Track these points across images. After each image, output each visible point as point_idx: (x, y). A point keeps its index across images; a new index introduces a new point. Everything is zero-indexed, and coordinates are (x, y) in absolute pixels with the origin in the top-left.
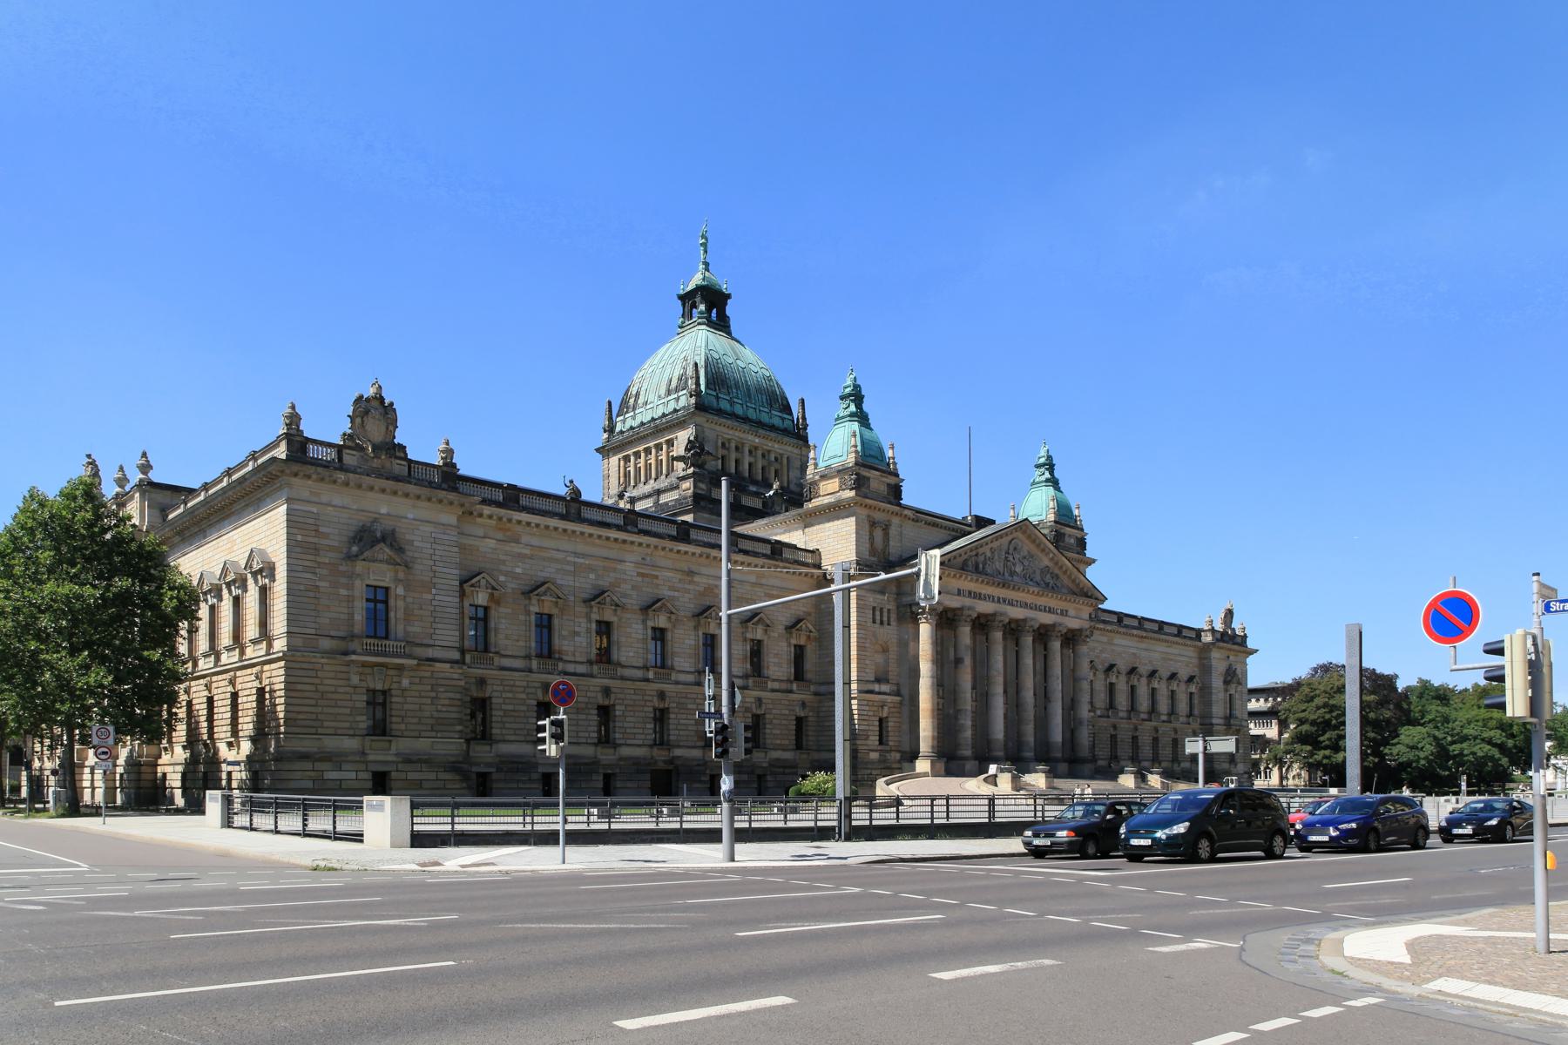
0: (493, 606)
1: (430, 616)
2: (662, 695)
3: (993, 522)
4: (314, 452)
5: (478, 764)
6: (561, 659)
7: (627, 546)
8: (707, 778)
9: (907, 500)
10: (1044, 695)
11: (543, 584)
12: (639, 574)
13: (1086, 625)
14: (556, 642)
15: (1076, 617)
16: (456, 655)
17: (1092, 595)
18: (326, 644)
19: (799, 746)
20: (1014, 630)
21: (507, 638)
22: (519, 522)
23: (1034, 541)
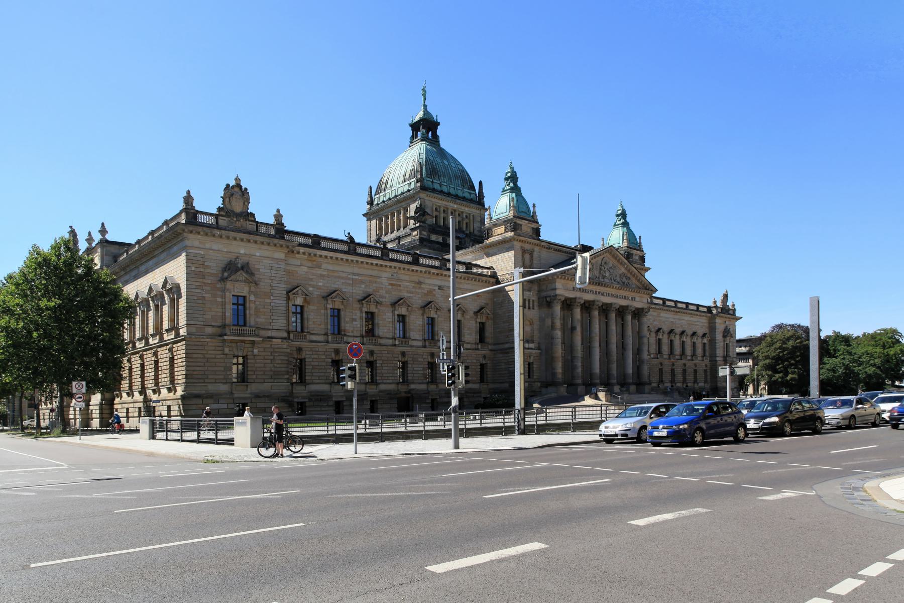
0: (306, 305)
1: (270, 314)
2: (403, 354)
3: (592, 248)
4: (202, 219)
6: (345, 335)
7: (383, 269)
8: (429, 401)
9: (543, 237)
10: (622, 347)
11: (335, 291)
12: (391, 284)
13: (645, 306)
15: (640, 302)
16: (285, 335)
17: (649, 289)
18: (209, 330)
19: (482, 380)
20: (605, 309)
21: (314, 323)
22: (321, 256)
23: (616, 259)
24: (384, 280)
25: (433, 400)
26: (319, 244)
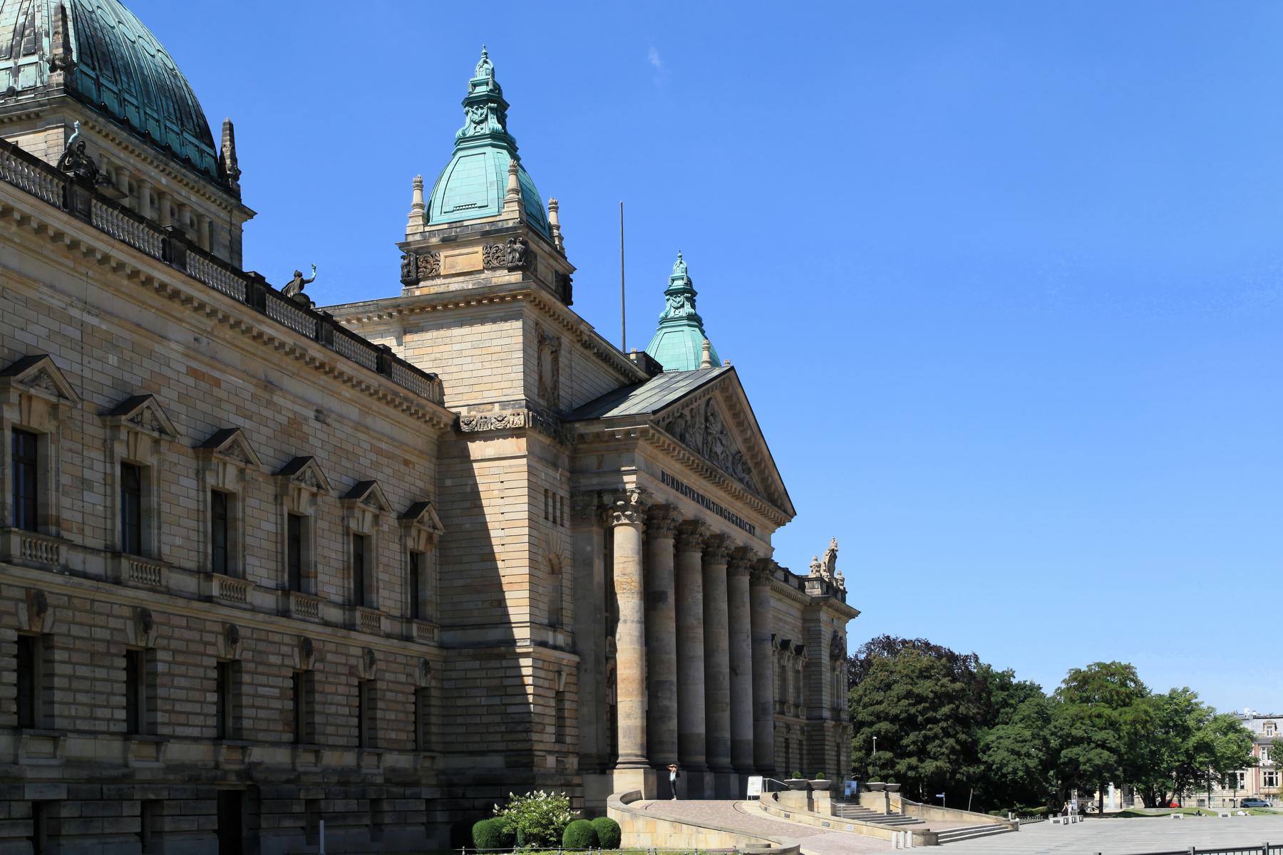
2: (232, 635)
7: (175, 307)
11: (28, 361)
24: (173, 351)
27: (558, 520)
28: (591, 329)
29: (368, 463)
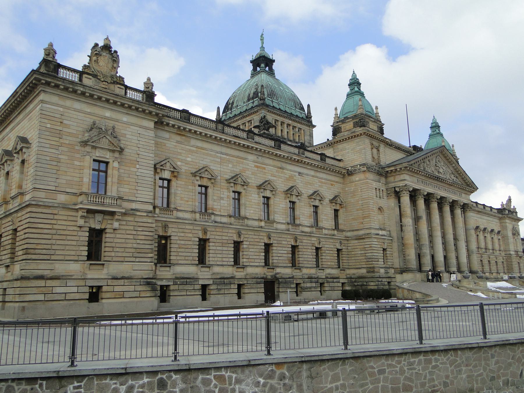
0: (174, 180)
5: (162, 279)
12: (257, 167)
14: (210, 203)
16: (151, 208)
22: (190, 130)
23: (445, 157)
25: (297, 284)
26: (189, 120)
27: (382, 197)
28: (390, 140)
29: (318, 186)
